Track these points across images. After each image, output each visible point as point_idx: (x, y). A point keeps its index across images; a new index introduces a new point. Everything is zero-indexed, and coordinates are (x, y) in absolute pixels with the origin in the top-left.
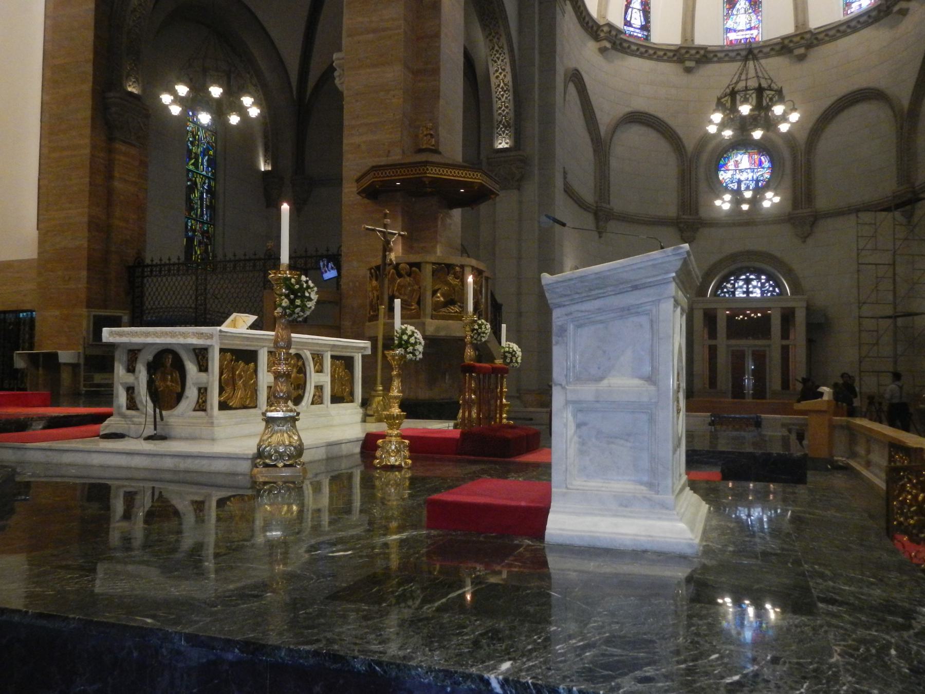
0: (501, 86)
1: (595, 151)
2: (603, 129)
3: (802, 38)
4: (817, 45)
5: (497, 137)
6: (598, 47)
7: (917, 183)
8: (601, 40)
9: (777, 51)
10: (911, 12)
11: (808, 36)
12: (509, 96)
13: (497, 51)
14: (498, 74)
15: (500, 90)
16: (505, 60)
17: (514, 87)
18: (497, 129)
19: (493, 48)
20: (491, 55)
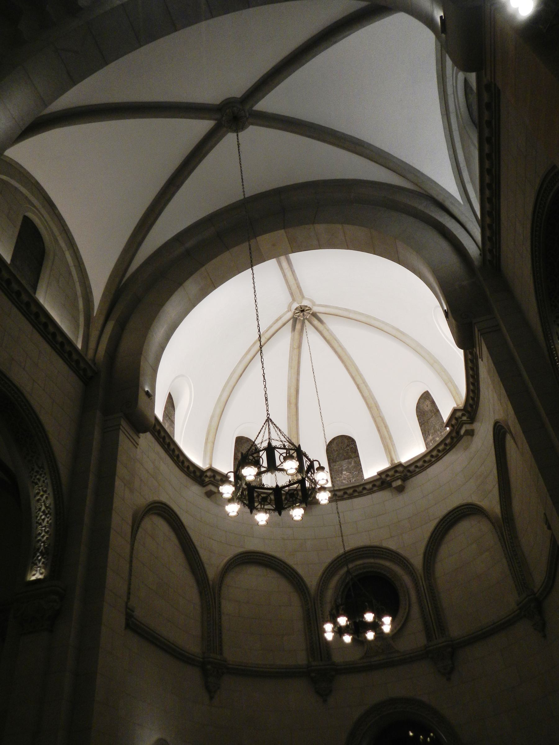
1: (201, 593)
2: (212, 573)
3: (396, 472)
4: (412, 477)
6: (205, 491)
7: (536, 590)
9: (378, 487)
10: (476, 432)
11: (400, 469)
12: (50, 519)
13: (37, 472)
14: (38, 497)
15: (41, 514)
16: (46, 481)
18: (34, 557)
19: (33, 469)
20: (31, 477)
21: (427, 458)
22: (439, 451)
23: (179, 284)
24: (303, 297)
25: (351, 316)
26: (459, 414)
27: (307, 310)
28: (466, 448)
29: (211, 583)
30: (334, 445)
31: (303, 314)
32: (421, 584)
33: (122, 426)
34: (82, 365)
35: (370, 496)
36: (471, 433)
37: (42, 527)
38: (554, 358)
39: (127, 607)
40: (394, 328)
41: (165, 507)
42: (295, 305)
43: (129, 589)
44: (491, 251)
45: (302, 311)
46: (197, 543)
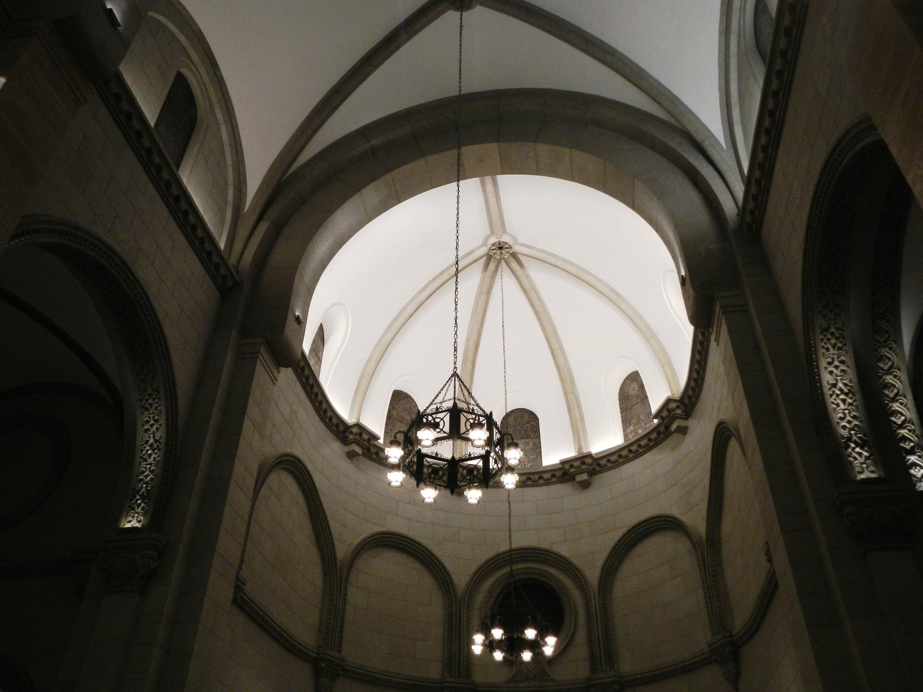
0: (150, 443)
1: (325, 574)
2: (342, 551)
3: (583, 463)
4: (600, 472)
5: (128, 512)
8: (350, 443)
10: (689, 431)
11: (589, 461)
12: (158, 456)
13: (150, 395)
15: (148, 448)
16: (159, 408)
17: (167, 444)
18: (132, 500)
19: (145, 391)
20: (142, 401)
21: (624, 453)
22: (640, 446)
23: (357, 190)
24: (504, 231)
25: (559, 264)
26: (673, 405)
27: (506, 248)
28: (673, 449)
29: (339, 564)
30: (511, 419)
31: (501, 252)
32: (593, 603)
33: (261, 354)
34: (222, 271)
35: (545, 488)
36: (683, 431)
37: (146, 465)
38: (811, 355)
39: (237, 579)
40: (608, 286)
41: (296, 461)
42: (493, 240)
43: (243, 556)
44: (752, 213)
45: (501, 248)
46: (328, 513)
